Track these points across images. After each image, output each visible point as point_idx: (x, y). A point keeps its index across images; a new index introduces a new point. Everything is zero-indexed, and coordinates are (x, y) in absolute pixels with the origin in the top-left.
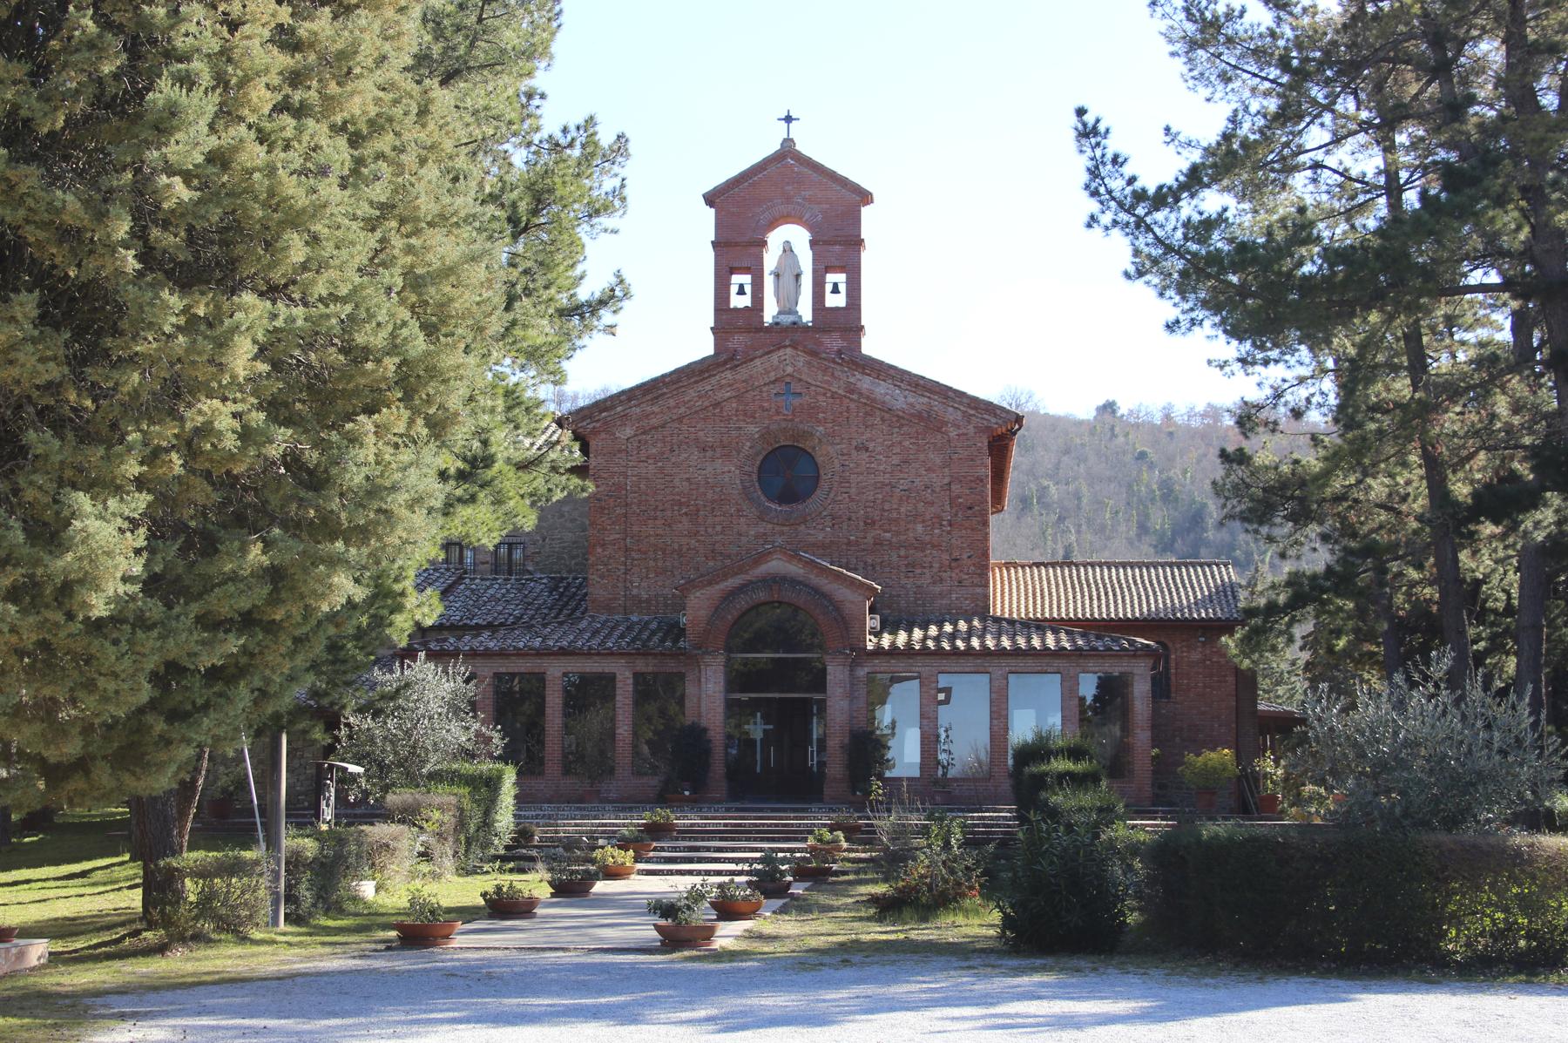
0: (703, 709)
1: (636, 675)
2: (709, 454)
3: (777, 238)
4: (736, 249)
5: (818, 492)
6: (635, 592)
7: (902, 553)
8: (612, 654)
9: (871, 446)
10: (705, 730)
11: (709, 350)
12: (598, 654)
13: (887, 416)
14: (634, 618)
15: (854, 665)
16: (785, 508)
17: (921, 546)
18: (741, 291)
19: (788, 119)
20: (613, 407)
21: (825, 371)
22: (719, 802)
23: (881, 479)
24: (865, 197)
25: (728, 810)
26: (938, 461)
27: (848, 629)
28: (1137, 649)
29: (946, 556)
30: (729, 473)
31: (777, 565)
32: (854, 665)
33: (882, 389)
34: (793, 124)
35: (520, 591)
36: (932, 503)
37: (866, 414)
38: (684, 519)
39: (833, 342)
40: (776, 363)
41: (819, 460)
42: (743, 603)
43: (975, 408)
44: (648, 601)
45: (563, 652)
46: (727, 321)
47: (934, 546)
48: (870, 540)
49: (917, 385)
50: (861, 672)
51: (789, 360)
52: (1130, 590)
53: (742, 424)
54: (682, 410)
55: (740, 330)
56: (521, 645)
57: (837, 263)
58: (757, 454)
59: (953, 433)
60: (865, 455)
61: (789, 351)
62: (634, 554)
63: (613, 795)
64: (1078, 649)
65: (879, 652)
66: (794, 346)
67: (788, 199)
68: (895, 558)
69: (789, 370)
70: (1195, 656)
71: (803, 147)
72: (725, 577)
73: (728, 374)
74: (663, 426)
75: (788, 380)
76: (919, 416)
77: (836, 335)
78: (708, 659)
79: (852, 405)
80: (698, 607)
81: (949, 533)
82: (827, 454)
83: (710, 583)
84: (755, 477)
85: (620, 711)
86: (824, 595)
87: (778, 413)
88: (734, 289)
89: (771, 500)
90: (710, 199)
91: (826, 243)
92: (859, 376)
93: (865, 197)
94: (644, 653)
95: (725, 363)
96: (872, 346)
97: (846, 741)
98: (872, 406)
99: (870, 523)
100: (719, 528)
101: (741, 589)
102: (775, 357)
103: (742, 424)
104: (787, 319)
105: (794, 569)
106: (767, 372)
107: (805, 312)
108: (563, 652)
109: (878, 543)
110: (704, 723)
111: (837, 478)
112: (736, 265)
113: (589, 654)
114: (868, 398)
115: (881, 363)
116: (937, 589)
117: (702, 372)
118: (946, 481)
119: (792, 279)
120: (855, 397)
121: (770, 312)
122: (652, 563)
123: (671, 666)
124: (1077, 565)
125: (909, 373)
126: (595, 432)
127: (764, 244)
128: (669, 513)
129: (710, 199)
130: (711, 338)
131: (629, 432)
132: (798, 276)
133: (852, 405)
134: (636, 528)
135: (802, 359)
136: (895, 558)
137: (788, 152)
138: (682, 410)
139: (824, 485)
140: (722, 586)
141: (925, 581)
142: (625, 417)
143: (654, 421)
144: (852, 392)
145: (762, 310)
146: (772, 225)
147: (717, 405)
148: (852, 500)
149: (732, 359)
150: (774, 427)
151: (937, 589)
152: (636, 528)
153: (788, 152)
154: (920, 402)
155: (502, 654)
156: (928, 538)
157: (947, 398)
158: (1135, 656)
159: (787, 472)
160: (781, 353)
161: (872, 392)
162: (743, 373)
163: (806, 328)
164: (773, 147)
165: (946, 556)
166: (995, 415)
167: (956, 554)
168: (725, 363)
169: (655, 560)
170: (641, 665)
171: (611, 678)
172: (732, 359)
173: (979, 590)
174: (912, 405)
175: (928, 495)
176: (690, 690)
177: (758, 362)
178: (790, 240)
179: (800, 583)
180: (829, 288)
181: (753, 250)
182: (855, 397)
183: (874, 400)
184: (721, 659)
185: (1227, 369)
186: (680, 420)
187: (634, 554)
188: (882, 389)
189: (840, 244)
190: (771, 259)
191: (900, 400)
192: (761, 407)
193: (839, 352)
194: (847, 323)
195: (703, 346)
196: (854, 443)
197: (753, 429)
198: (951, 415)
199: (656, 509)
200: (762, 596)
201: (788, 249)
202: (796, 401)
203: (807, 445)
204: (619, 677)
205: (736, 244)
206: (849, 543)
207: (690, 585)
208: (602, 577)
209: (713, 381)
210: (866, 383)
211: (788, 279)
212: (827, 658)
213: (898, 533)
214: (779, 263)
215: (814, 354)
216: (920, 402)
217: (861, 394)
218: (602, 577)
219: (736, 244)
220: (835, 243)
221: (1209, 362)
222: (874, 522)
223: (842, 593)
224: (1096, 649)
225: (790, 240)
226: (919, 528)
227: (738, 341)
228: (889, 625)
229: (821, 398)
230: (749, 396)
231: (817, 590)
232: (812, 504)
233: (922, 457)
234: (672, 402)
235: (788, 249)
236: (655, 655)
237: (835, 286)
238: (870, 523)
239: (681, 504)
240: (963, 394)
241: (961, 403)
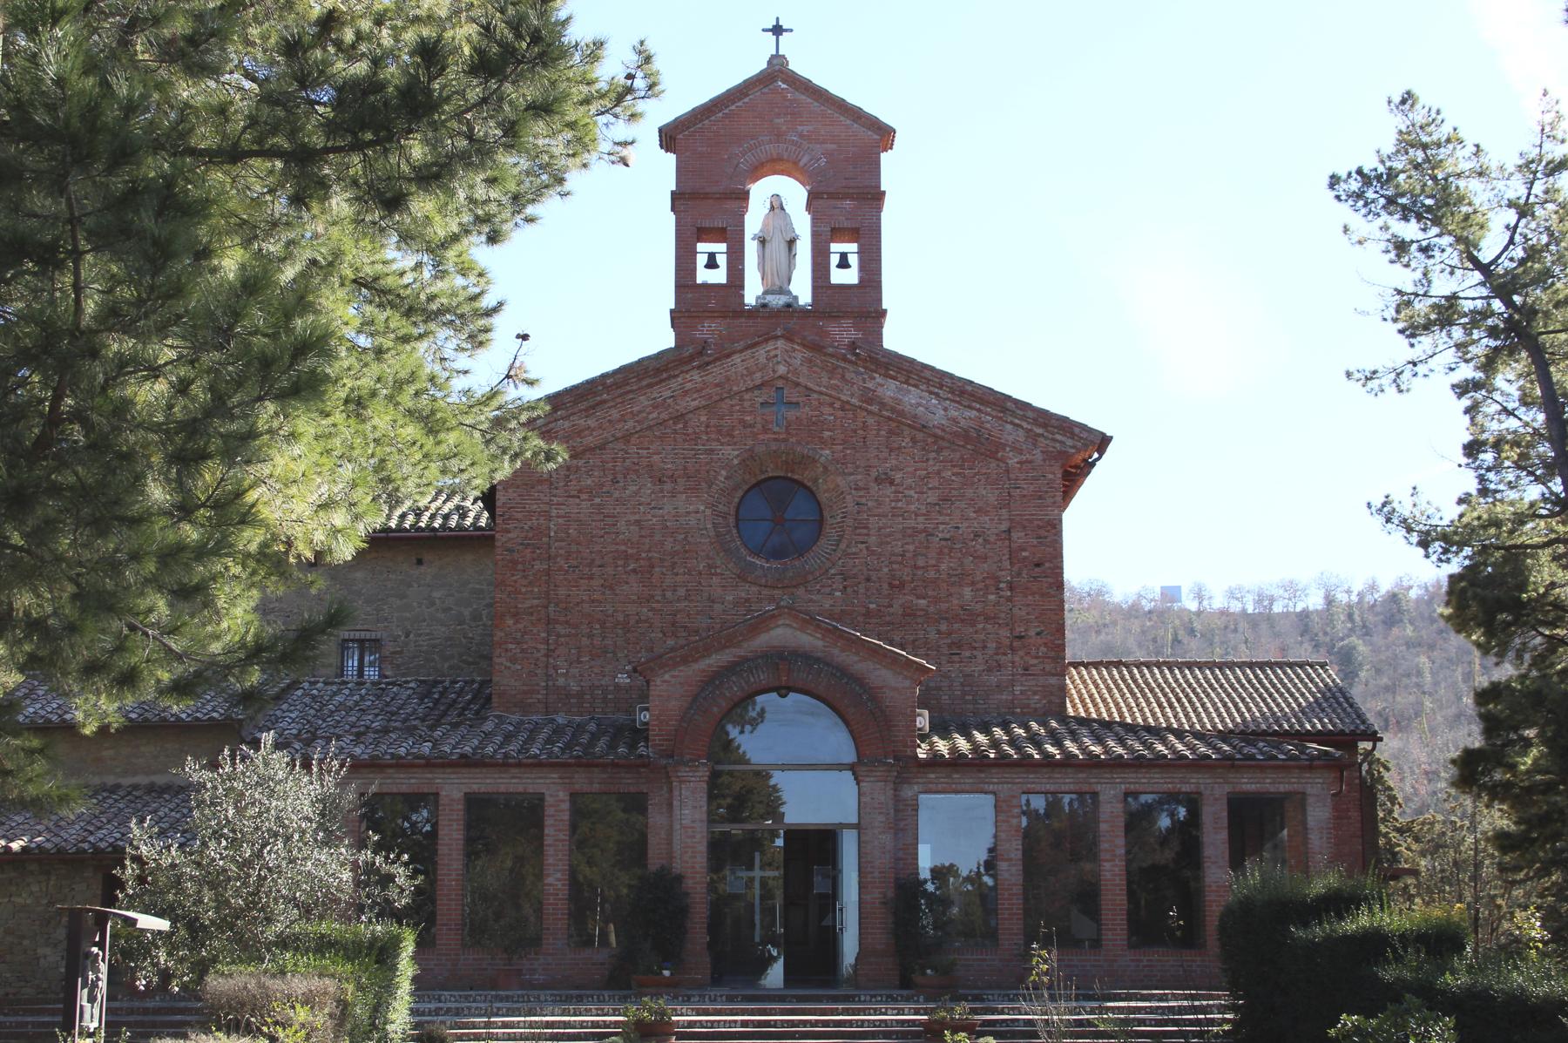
0: (677, 847)
1: (574, 796)
2: (668, 486)
3: (761, 192)
4: (705, 208)
5: (822, 541)
6: (561, 682)
7: (944, 627)
8: (540, 765)
9: (898, 476)
10: (679, 878)
11: (665, 339)
12: (519, 765)
13: (920, 436)
14: (560, 720)
16: (775, 565)
18: (712, 264)
19: (777, 30)
21: (832, 372)
23: (911, 523)
24: (883, 135)
25: (730, 999)
26: (992, 499)
28: (1312, 758)
29: (1005, 633)
30: (694, 512)
33: (913, 398)
34: (784, 38)
35: (378, 697)
36: (985, 558)
37: (891, 432)
39: (843, 333)
40: (762, 360)
41: (823, 497)
43: (1045, 426)
44: (580, 695)
46: (692, 305)
47: (987, 619)
48: (897, 608)
49: (963, 392)
51: (780, 357)
52: (1208, 695)
53: (715, 445)
54: (630, 424)
55: (711, 314)
56: (402, 751)
57: (847, 224)
58: (735, 489)
59: (1013, 461)
60: (889, 490)
61: (780, 343)
62: (559, 628)
64: (1229, 758)
65: (935, 760)
66: (789, 338)
67: (779, 136)
69: (782, 369)
71: (798, 66)
72: (707, 651)
73: (696, 376)
74: (602, 447)
75: (780, 384)
76: (965, 435)
77: (847, 323)
78: (684, 772)
79: (871, 421)
81: (1009, 599)
83: (685, 661)
84: (732, 520)
85: (549, 851)
86: (859, 681)
87: (765, 430)
88: (702, 260)
89: (756, 553)
91: (833, 196)
92: (879, 379)
93: (883, 135)
94: (586, 763)
95: (692, 358)
96: (900, 335)
97: (890, 894)
98: (897, 420)
99: (897, 586)
100: (681, 592)
101: (732, 668)
102: (761, 353)
103: (715, 445)
104: (777, 301)
105: (808, 640)
106: (751, 374)
107: (802, 289)
109: (909, 613)
110: (677, 867)
111: (849, 521)
112: (707, 224)
113: (505, 765)
114: (893, 410)
115: (912, 361)
116: (994, 679)
117: (658, 371)
118: (1004, 527)
119: (784, 247)
120: (875, 408)
121: (753, 291)
122: (585, 641)
124: (1127, 666)
125: (951, 376)
127: (744, 196)
128: (610, 570)
132: (791, 243)
133: (871, 421)
134: (562, 592)
135: (800, 356)
136: (933, 636)
137: (777, 70)
138: (630, 424)
139: (830, 532)
140: (703, 664)
143: (590, 440)
144: (870, 401)
145: (742, 287)
146: (757, 173)
147: (679, 417)
148: (873, 553)
149: (700, 353)
150: (760, 449)
151: (994, 679)
152: (562, 592)
153: (777, 70)
154: (966, 416)
156: (979, 607)
157: (1004, 410)
158: (1310, 768)
160: (770, 346)
161: (899, 402)
162: (716, 372)
163: (803, 312)
164: (757, 65)
165: (1005, 632)
166: (1073, 435)
167: (1020, 629)
168: (692, 358)
169: (591, 636)
171: (541, 797)
172: (700, 353)
173: (1053, 680)
174: (954, 420)
177: (737, 358)
178: (775, 200)
179: (818, 660)
180: (835, 260)
181: (731, 205)
182: (875, 408)
183: (902, 413)
184: (703, 773)
185: (1374, 384)
186: (626, 438)
187: (559, 628)
188: (913, 398)
190: (754, 220)
191: (938, 413)
192: (742, 421)
193: (853, 346)
194: (863, 304)
195: (655, 335)
196: (874, 473)
197: (730, 453)
198: (1010, 434)
199: (590, 565)
201: (777, 206)
202: (791, 414)
203: (805, 476)
204: (549, 800)
205: (706, 196)
208: (513, 660)
209: (674, 384)
210: (889, 389)
211: (777, 247)
213: (937, 600)
214: (765, 224)
215: (816, 348)
216: (966, 416)
217: (882, 405)
218: (513, 660)
219: (706, 196)
220: (846, 196)
221: (1349, 375)
222: (902, 585)
223: (881, 676)
224: (1252, 757)
225: (775, 200)
226: (967, 592)
227: (709, 330)
228: (941, 728)
229: (827, 410)
230: (724, 406)
231: (843, 672)
233: (970, 493)
235: (777, 206)
236: (604, 766)
237: (844, 256)
238: (897, 586)
239: (627, 557)
240: (1026, 406)
241: (1024, 418)
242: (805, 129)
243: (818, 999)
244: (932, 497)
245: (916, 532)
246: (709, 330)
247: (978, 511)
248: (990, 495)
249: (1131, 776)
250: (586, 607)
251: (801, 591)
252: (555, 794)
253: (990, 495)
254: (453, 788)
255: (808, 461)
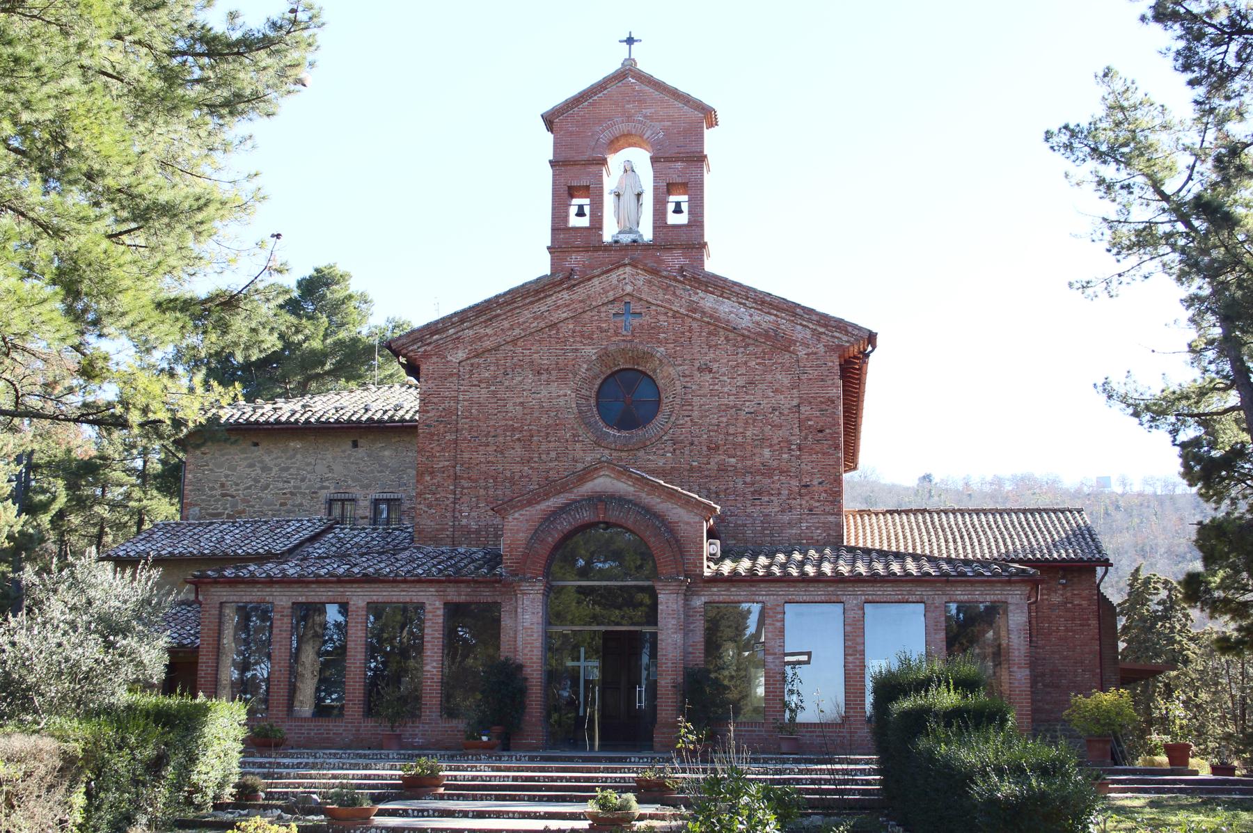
0: (520, 643)
1: (446, 604)
2: (544, 377)
3: (616, 161)
4: (575, 173)
5: (659, 417)
6: (464, 522)
7: (748, 479)
8: (420, 581)
9: (715, 366)
10: (520, 667)
11: (545, 270)
12: (405, 581)
13: (731, 335)
14: (461, 550)
15: (689, 593)
16: (625, 433)
17: (768, 471)
19: (630, 41)
20: (445, 329)
21: (666, 289)
22: (535, 749)
23: (725, 401)
24: (708, 115)
25: (532, 759)
26: (786, 382)
28: (1012, 575)
29: (795, 483)
30: (564, 396)
31: (604, 483)
32: (689, 593)
33: (725, 307)
34: (635, 46)
35: (384, 539)
37: (710, 333)
38: (518, 446)
39: (675, 260)
40: (615, 282)
41: (660, 383)
42: (565, 525)
43: (825, 326)
44: (478, 532)
45: (367, 580)
46: (564, 241)
47: (782, 472)
48: (713, 465)
49: (763, 302)
50: (698, 602)
51: (628, 279)
52: (985, 533)
53: (578, 346)
54: (517, 331)
55: (577, 249)
56: (323, 572)
57: (679, 180)
58: (595, 378)
59: (802, 352)
60: (708, 377)
61: (628, 269)
62: (465, 483)
63: (419, 740)
64: (946, 575)
65: (718, 579)
66: (634, 265)
67: (629, 118)
68: (740, 485)
69: (629, 289)
70: (1056, 599)
71: (644, 66)
72: (547, 496)
73: (565, 295)
74: (496, 349)
75: (627, 299)
76: (766, 335)
77: (677, 253)
78: (525, 586)
79: (695, 325)
80: (517, 528)
81: (798, 457)
82: (668, 376)
83: (530, 503)
84: (593, 402)
85: (428, 646)
86: (656, 516)
87: (616, 334)
88: (573, 210)
90: (550, 120)
91: (668, 159)
92: (701, 294)
93: (708, 115)
94: (454, 580)
95: (562, 282)
96: (719, 261)
97: (680, 680)
98: (715, 325)
99: (713, 448)
100: (553, 454)
101: (564, 509)
102: (613, 277)
103: (578, 346)
104: (626, 239)
105: (623, 487)
106: (606, 292)
107: (646, 232)
108: (367, 580)
109: (722, 468)
110: (520, 658)
111: (678, 400)
112: (575, 183)
113: (395, 581)
114: (711, 316)
115: (725, 280)
116: (786, 518)
117: (537, 292)
118: (795, 402)
119: (634, 199)
120: (698, 316)
121: (610, 232)
122: (482, 492)
123: (486, 595)
124: (930, 513)
125: (755, 291)
126: (426, 355)
127: (603, 162)
128: (501, 439)
129: (550, 120)
130: (547, 257)
131: (461, 355)
132: (639, 195)
133: (695, 325)
134: (466, 455)
135: (642, 277)
136: (740, 485)
137: (628, 72)
138: (517, 331)
139: (665, 409)
140: (543, 506)
141: (773, 509)
142: (457, 339)
143: (487, 344)
144: (694, 311)
145: (601, 228)
146: (615, 144)
147: (553, 326)
148: (695, 424)
149: (568, 278)
150: (612, 348)
151: (786, 518)
152: (466, 455)
153: (628, 72)
154: (766, 320)
155: (301, 581)
156: (775, 464)
157: (795, 315)
158: (1009, 582)
159: (626, 396)
160: (621, 271)
161: (716, 311)
162: (581, 292)
163: (647, 247)
165: (795, 483)
166: (847, 333)
167: (806, 480)
168: (562, 282)
169: (486, 488)
170: (456, 595)
171: (421, 606)
172: (568, 278)
173: (831, 519)
174: (758, 323)
175: (775, 418)
176: (506, 622)
177: (596, 281)
179: (630, 501)
180: (671, 207)
181: (593, 169)
182: (698, 316)
183: (718, 319)
184: (540, 587)
185: (1089, 291)
186: (514, 342)
187: (465, 483)
188: (725, 307)
189: (682, 165)
190: (611, 180)
191: (745, 318)
192: (599, 328)
193: (681, 270)
194: (690, 241)
195: (540, 266)
196: (697, 364)
197: (591, 351)
198: (800, 333)
199: (486, 436)
200: (586, 516)
201: (629, 169)
202: (636, 322)
203: (647, 368)
204: (428, 608)
205: (575, 163)
206: (691, 469)
208: (430, 506)
209: (549, 301)
210: (708, 301)
211: (629, 198)
212: (658, 585)
213: (744, 458)
214: (620, 183)
215: (654, 272)
216: (766, 320)
217: (704, 313)
218: (430, 506)
219: (575, 163)
220: (677, 160)
221: (1070, 285)
222: (717, 447)
223: (676, 513)
224: (964, 574)
226: (767, 452)
227: (575, 260)
229: (662, 318)
231: (647, 511)
232: (653, 429)
233: (769, 377)
234: (506, 324)
235: (629, 169)
236: (468, 582)
237: (678, 204)
238: (713, 448)
239: (514, 429)
240: (811, 311)
241: (810, 320)
242: (648, 112)
243: (571, 759)
244: (741, 381)
245: (728, 407)
246: (575, 260)
247: (776, 391)
250: (483, 467)
251: (641, 453)
252: (433, 604)
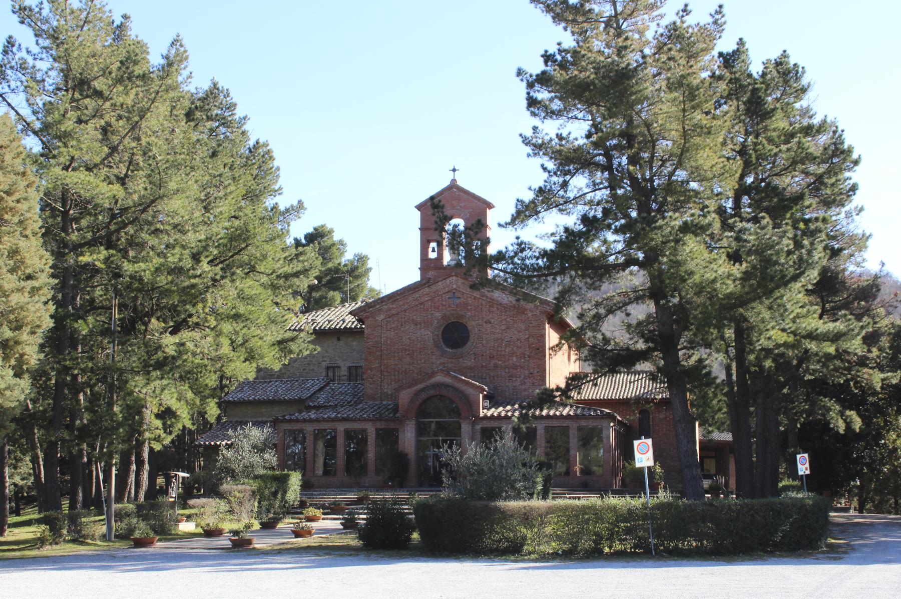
10: (406, 455)
15: (474, 424)
17: (515, 367)
18: (433, 251)
19: (454, 170)
20: (375, 306)
22: (413, 487)
26: (523, 327)
27: (472, 407)
29: (527, 372)
30: (427, 335)
31: (439, 378)
32: (474, 424)
36: (520, 347)
38: (408, 357)
41: (469, 328)
42: (424, 396)
44: (391, 395)
45: (344, 420)
46: (427, 265)
47: (521, 367)
48: (492, 364)
50: (478, 427)
56: (326, 416)
59: (530, 314)
60: (489, 325)
63: (367, 484)
68: (503, 373)
69: (455, 286)
70: (662, 416)
71: (461, 183)
72: (416, 384)
73: (427, 290)
74: (398, 314)
78: (408, 422)
80: (404, 397)
82: (471, 325)
83: (409, 387)
86: (462, 393)
88: (430, 249)
89: (448, 346)
90: (419, 207)
93: (490, 206)
94: (379, 419)
95: (425, 284)
99: (492, 357)
101: (423, 390)
102: (448, 281)
105: (447, 380)
108: (344, 420)
109: (496, 366)
110: (406, 451)
112: (430, 238)
116: (523, 387)
117: (414, 289)
123: (392, 425)
126: (367, 317)
129: (419, 207)
130: (419, 272)
131: (382, 317)
136: (503, 373)
137: (453, 187)
139: (471, 339)
140: (415, 388)
141: (517, 384)
142: (380, 310)
143: (393, 312)
151: (523, 387)
153: (453, 187)
155: (317, 420)
159: (455, 335)
162: (434, 288)
164: (446, 183)
165: (527, 372)
170: (380, 425)
175: (518, 343)
176: (401, 436)
177: (440, 283)
184: (413, 422)
186: (405, 311)
195: (414, 276)
197: (438, 315)
200: (432, 392)
202: (458, 301)
203: (464, 321)
206: (482, 366)
207: (400, 388)
209: (420, 292)
212: (461, 421)
213: (505, 362)
223: (470, 391)
226: (515, 359)
227: (431, 274)
228: (495, 404)
230: (436, 299)
232: (466, 349)
234: (401, 303)
238: (492, 357)
239: (406, 350)
242: (462, 205)
244: (503, 327)
245: (498, 339)
246: (431, 274)
247: (519, 332)
248: (522, 326)
249: (546, 421)
250: (393, 367)
251: (461, 360)
252: (371, 430)
253: (522, 326)
254: (341, 427)
255: (462, 316)
